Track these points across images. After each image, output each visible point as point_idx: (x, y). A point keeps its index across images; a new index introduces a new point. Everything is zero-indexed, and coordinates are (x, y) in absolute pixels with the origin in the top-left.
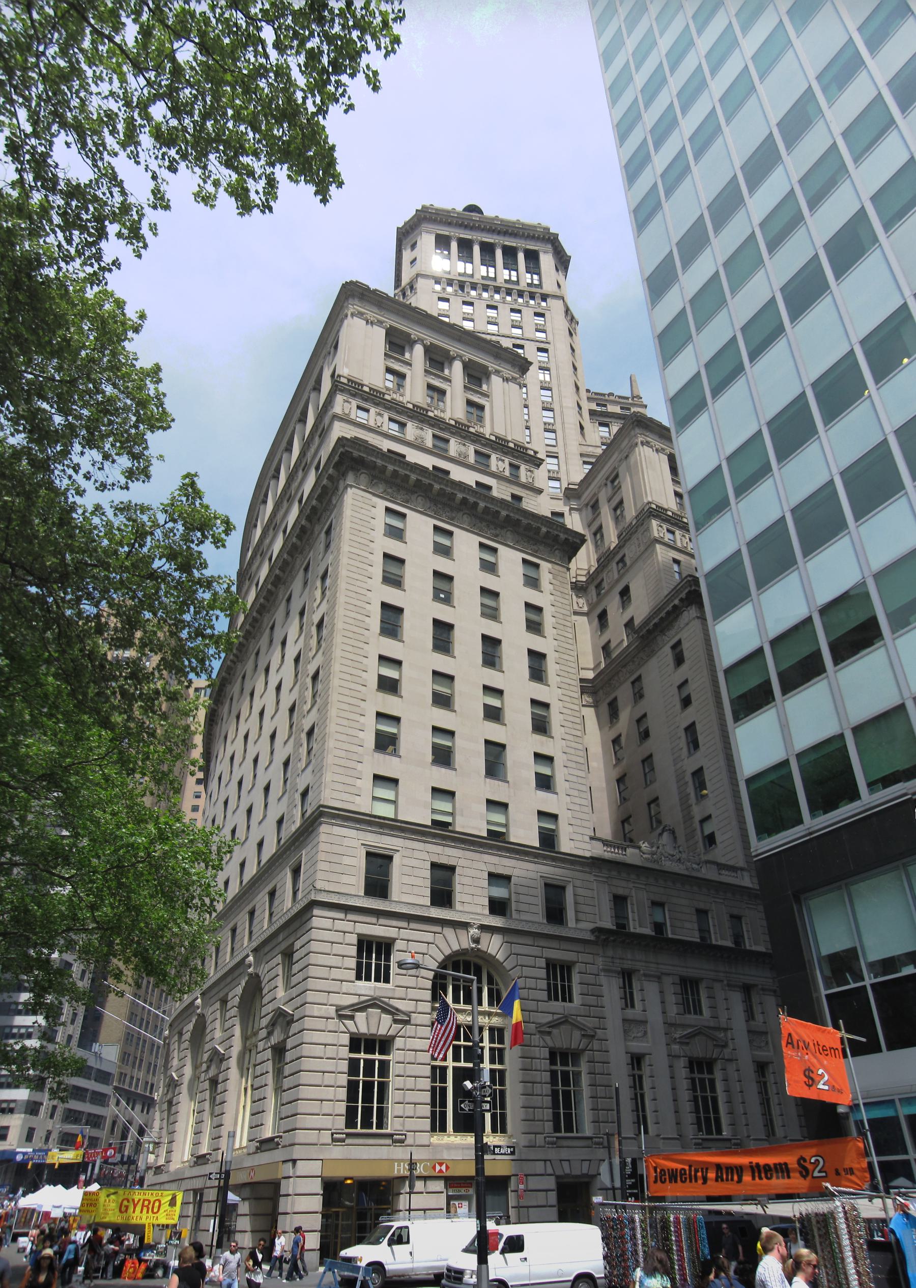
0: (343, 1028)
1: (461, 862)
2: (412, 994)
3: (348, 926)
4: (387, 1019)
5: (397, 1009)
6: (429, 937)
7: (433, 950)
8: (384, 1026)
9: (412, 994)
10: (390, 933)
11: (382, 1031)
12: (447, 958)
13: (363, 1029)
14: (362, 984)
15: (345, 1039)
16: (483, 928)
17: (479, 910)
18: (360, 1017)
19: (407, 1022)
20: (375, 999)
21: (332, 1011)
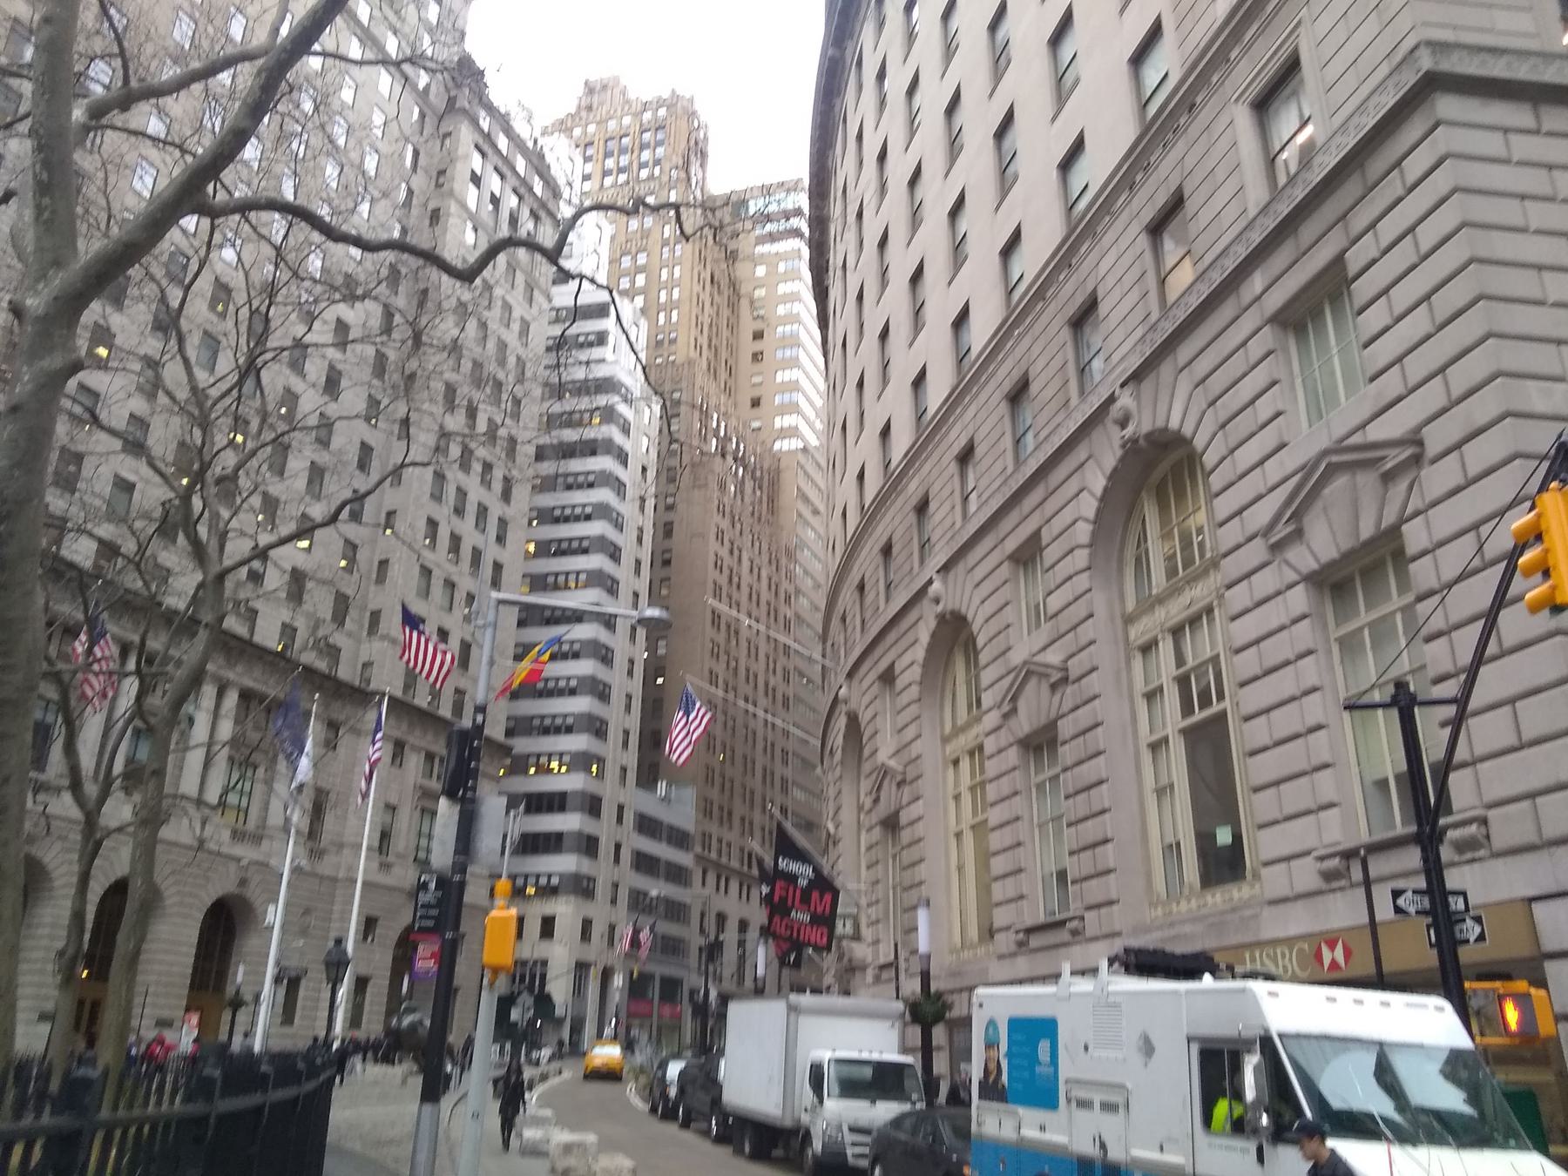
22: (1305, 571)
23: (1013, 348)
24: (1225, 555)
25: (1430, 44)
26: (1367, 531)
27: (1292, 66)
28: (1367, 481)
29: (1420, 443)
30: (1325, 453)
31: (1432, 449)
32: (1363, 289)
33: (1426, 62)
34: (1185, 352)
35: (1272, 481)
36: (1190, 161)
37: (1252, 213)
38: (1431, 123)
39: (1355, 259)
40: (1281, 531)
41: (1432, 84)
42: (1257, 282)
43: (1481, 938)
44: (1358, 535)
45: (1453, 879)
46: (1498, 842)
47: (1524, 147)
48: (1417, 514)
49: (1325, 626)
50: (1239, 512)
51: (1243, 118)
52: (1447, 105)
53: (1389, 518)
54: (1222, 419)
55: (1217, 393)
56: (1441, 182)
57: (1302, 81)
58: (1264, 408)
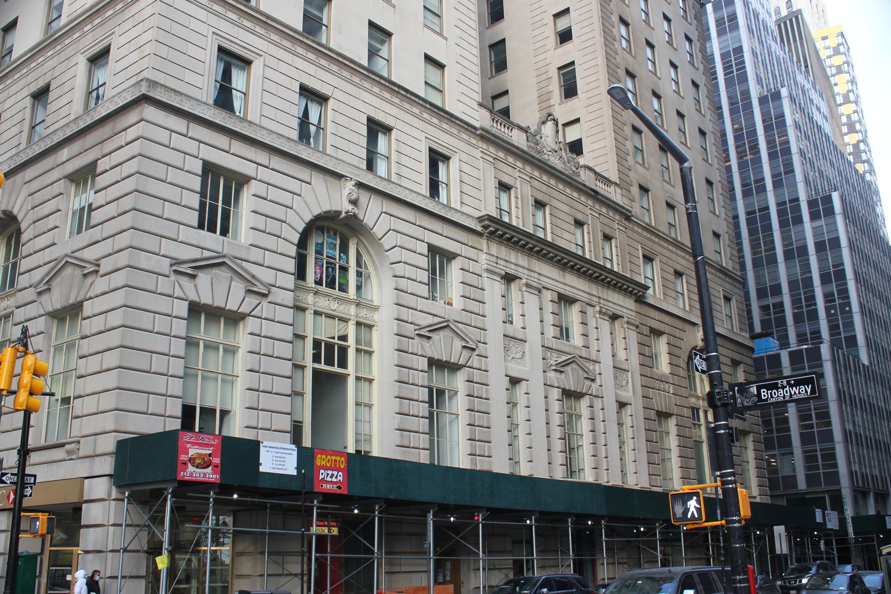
0: (178, 292)
1: (337, 94)
2: (271, 259)
3: (190, 146)
4: (239, 288)
5: (254, 277)
6: (294, 185)
7: (297, 203)
8: (234, 298)
9: (271, 259)
10: (247, 169)
11: (232, 306)
12: (318, 218)
13: (206, 299)
14: (204, 233)
15: (182, 309)
16: (360, 185)
17: (355, 161)
18: (203, 278)
19: (265, 296)
20: (224, 256)
21: (164, 265)
22: (47, 310)
23: (27, 75)
24: (20, 291)
25: (147, 80)
26: (71, 301)
27: (106, 52)
28: (78, 272)
29: (99, 265)
30: (66, 256)
31: (102, 271)
32: (101, 181)
33: (144, 89)
34: (30, 173)
35: (46, 260)
36: (57, 72)
37: (72, 117)
38: (139, 118)
39: (102, 166)
40: (42, 287)
41: (144, 99)
42: (64, 154)
43: (31, 495)
44: (69, 300)
45: (28, 471)
46: (81, 454)
47: (178, 141)
48: (91, 298)
49: (50, 339)
50: (30, 271)
51: (82, 63)
52: (150, 112)
53: (80, 298)
54: (35, 218)
55: (37, 203)
56: (135, 148)
57: (107, 63)
58: (51, 222)
